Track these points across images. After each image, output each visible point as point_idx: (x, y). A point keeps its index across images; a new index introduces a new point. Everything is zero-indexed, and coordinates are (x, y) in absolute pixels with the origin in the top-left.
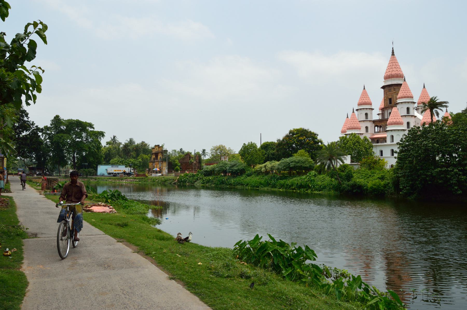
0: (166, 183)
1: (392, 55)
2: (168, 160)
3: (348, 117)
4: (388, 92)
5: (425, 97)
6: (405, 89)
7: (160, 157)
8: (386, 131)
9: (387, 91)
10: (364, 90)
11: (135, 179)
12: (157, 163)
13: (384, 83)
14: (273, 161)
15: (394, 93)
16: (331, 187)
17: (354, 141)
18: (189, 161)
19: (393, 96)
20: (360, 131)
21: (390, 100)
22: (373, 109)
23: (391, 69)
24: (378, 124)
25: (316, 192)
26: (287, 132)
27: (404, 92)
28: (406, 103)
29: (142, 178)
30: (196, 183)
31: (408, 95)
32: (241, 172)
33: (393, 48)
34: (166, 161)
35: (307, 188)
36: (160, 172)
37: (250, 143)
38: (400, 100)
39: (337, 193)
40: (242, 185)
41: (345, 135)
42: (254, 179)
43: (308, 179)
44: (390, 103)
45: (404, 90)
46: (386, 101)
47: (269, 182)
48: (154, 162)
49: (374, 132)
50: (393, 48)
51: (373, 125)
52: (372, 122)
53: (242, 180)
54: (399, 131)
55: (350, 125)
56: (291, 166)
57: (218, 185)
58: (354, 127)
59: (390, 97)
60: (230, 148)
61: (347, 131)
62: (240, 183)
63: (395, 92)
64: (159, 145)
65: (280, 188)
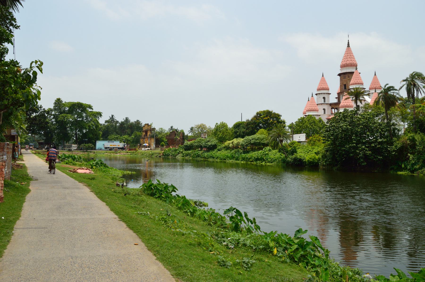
0: (153, 156)
1: (348, 46)
2: (155, 137)
3: (309, 100)
4: (343, 79)
6: (356, 77)
7: (149, 134)
9: (342, 78)
11: (127, 152)
12: (147, 139)
13: (340, 71)
14: (239, 138)
15: (348, 79)
18: (175, 137)
20: (317, 113)
21: (345, 85)
22: (330, 94)
23: (346, 59)
24: (334, 107)
26: (255, 114)
29: (133, 152)
30: (177, 156)
31: (359, 82)
32: (213, 148)
33: (348, 40)
34: (154, 137)
36: (149, 147)
37: (222, 123)
40: (213, 158)
42: (224, 153)
44: (345, 88)
45: (355, 78)
47: (234, 156)
48: (144, 138)
49: (330, 114)
50: (348, 40)
51: (330, 107)
52: (328, 106)
53: (214, 154)
55: (309, 108)
56: (252, 142)
57: (194, 158)
58: (312, 109)
59: (345, 83)
60: (210, 126)
61: (306, 112)
65: (242, 161)
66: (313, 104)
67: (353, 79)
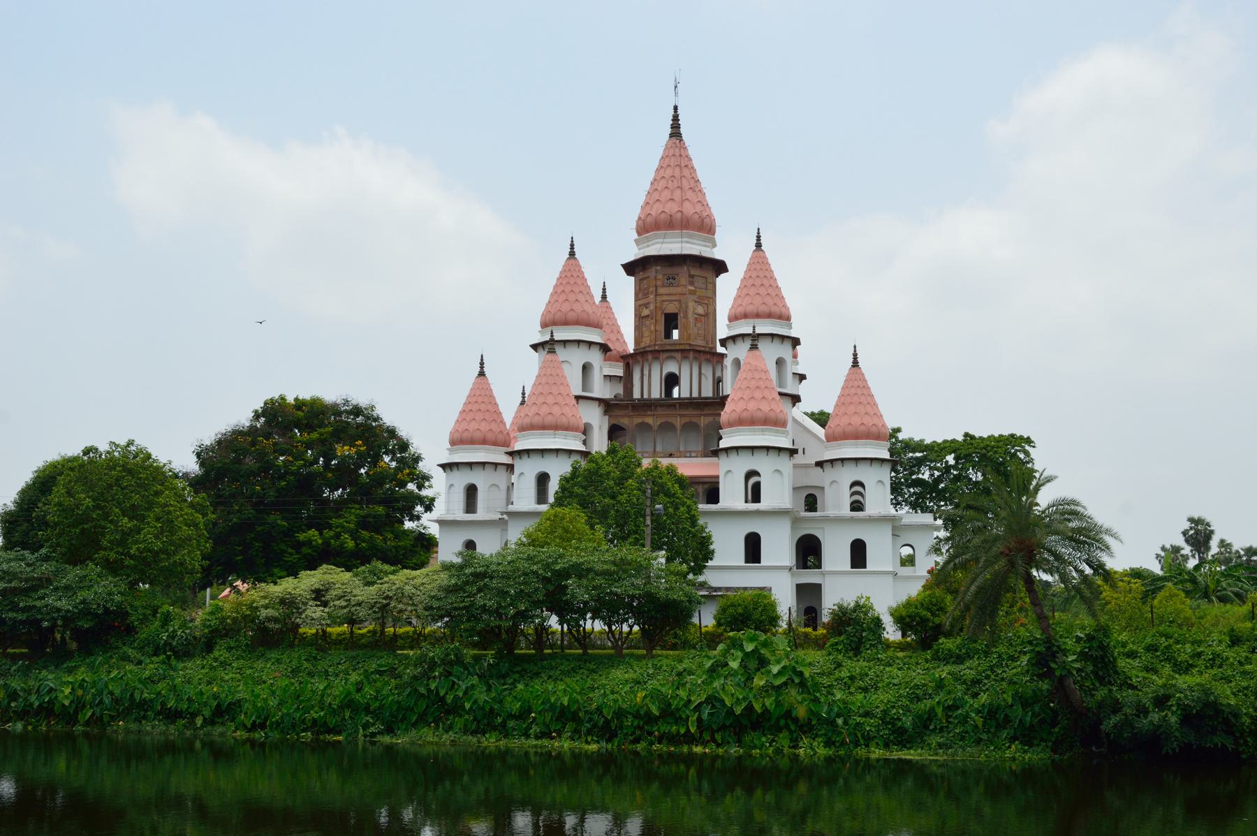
1: (671, 135)
4: (663, 286)
8: (716, 453)
10: (572, 261)
19: (687, 307)
33: (676, 108)
50: (676, 108)
55: (545, 410)
59: (671, 308)
62: (144, 705)
63: (693, 288)
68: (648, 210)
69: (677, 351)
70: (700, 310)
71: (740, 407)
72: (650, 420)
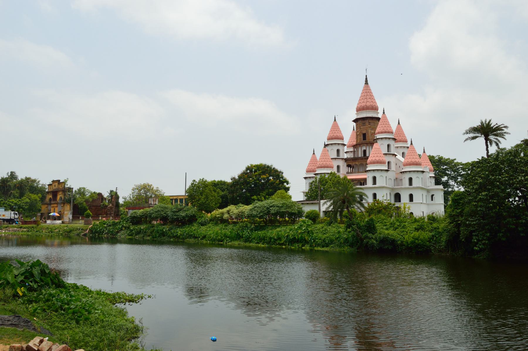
0: (71, 234)
1: (365, 84)
2: (73, 201)
4: (362, 126)
5: (401, 135)
7: (61, 198)
8: (367, 171)
9: (361, 125)
11: (21, 227)
12: (55, 205)
15: (369, 127)
16: (342, 242)
17: (334, 181)
18: (101, 204)
21: (364, 135)
23: (366, 100)
24: (350, 164)
25: (319, 248)
26: (243, 169)
27: (384, 126)
28: (387, 139)
29: (33, 227)
30: (119, 234)
31: (389, 130)
32: (191, 220)
33: (366, 76)
34: (70, 203)
35: (303, 242)
36: (59, 218)
38: (379, 136)
39: (352, 249)
40: (195, 237)
41: (315, 174)
42: (212, 230)
43: (305, 229)
44: (364, 138)
45: (383, 124)
46: (359, 136)
47: (241, 234)
48: (50, 204)
49: (346, 173)
50: (366, 76)
51: (345, 164)
52: (344, 161)
53: (194, 230)
54: (375, 171)
55: (322, 163)
56: (272, 212)
57: (156, 237)
58: (326, 165)
59: (364, 132)
60: (158, 188)
62: (191, 235)
64: (59, 181)
65: (258, 243)
66: (327, 157)
67: (381, 126)
68: (360, 104)
69: (365, 143)
70: (373, 132)
71: (374, 159)
72: (357, 163)
